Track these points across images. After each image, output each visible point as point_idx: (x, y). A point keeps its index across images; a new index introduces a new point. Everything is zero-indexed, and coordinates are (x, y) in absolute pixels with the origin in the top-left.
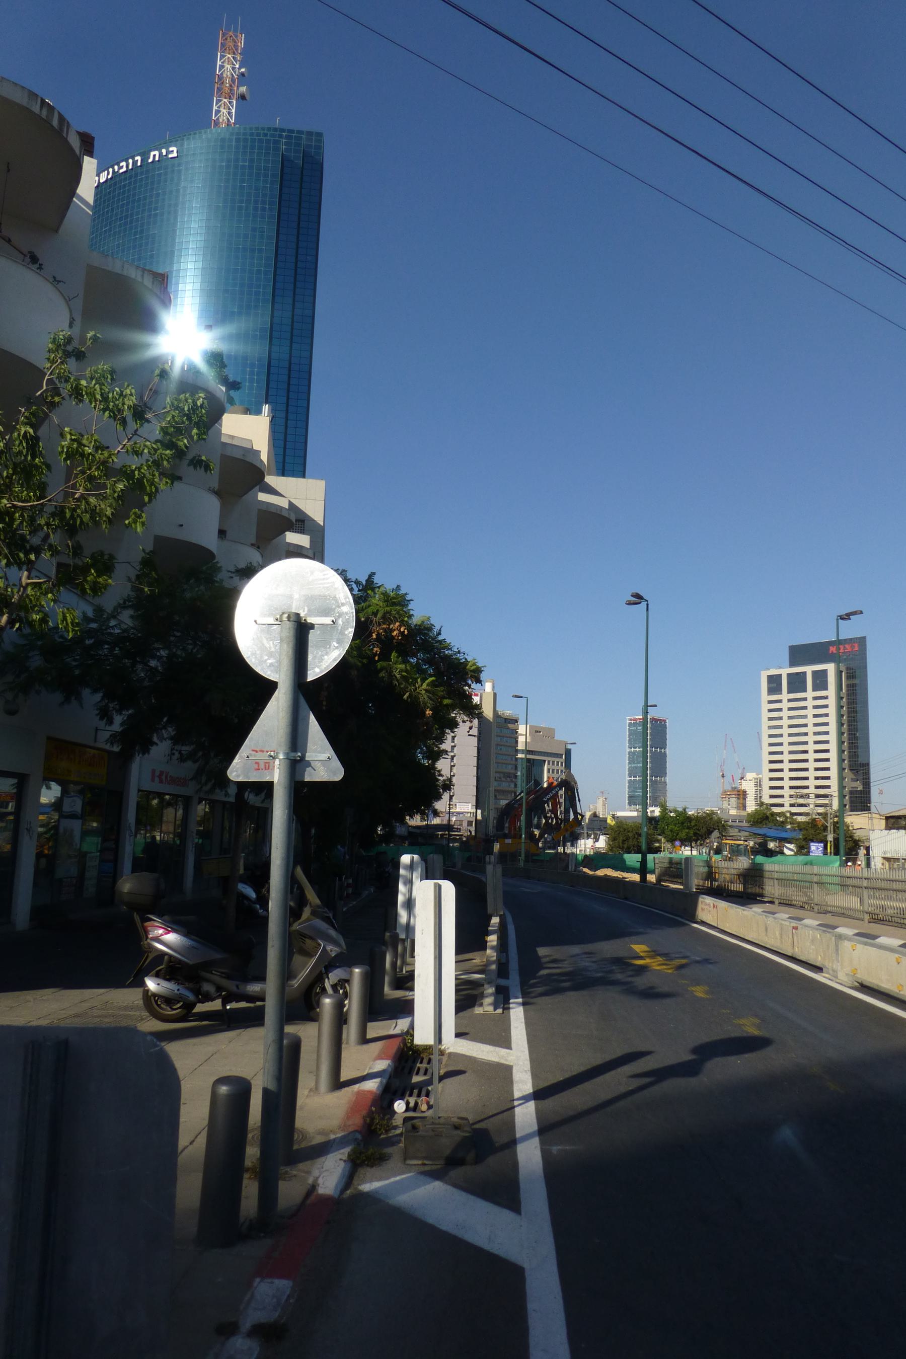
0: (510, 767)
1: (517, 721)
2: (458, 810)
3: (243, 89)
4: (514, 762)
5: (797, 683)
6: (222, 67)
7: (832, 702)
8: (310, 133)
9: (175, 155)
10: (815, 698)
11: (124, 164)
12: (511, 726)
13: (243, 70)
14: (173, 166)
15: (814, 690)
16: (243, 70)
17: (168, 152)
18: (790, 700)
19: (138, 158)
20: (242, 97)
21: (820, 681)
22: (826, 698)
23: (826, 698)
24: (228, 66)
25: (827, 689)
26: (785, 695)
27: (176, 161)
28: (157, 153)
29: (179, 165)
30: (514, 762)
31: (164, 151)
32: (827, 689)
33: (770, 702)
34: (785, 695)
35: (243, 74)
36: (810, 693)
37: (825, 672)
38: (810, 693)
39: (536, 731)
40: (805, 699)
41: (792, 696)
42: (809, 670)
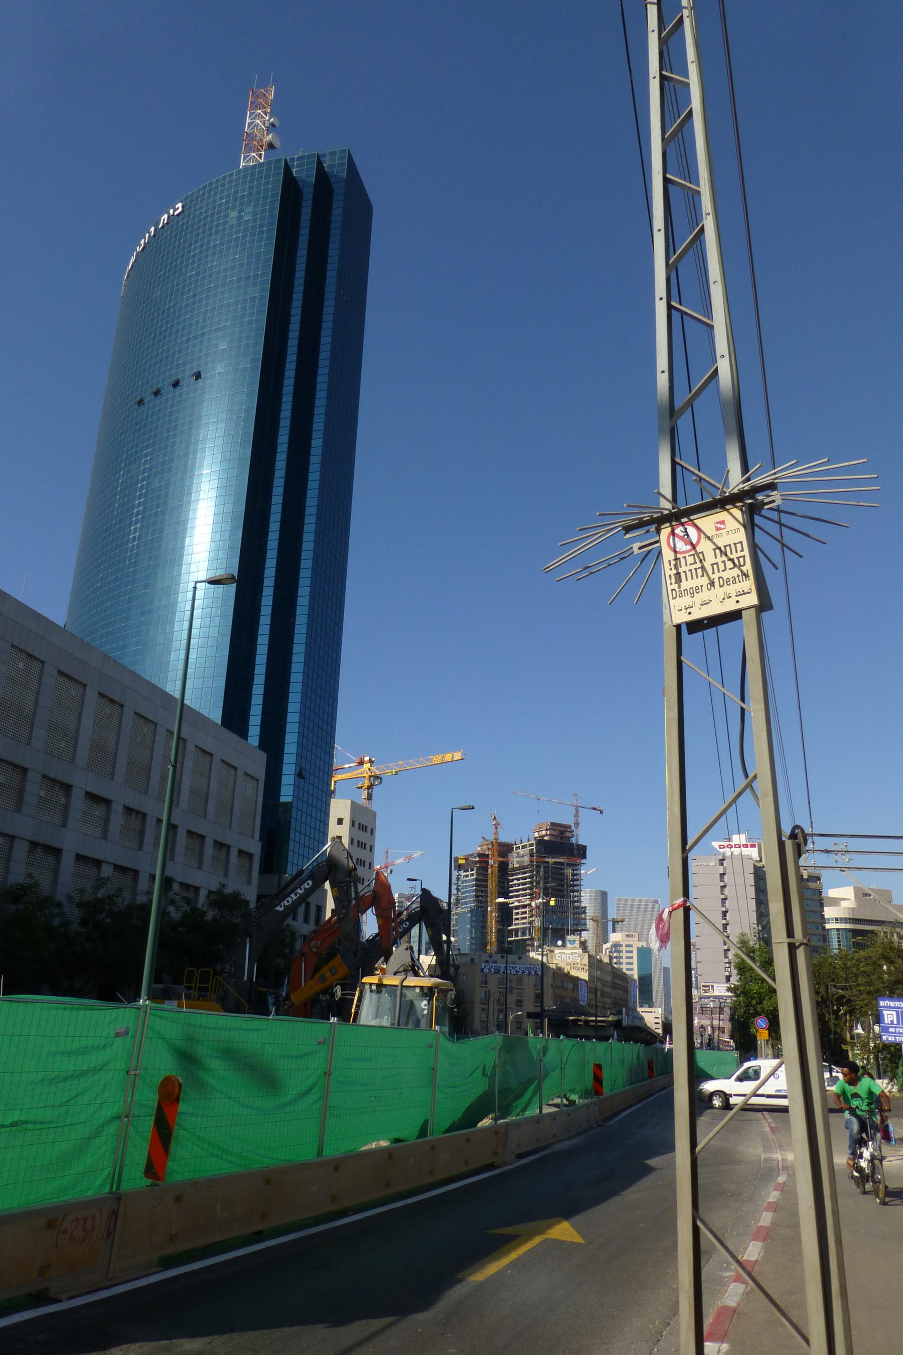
0: (816, 938)
1: (819, 878)
2: (716, 993)
3: (269, 138)
4: (820, 931)
6: (250, 124)
8: (333, 154)
9: (180, 210)
11: (143, 241)
12: (812, 885)
13: (272, 120)
14: (178, 222)
16: (272, 120)
17: (175, 210)
19: (152, 229)
20: (271, 146)
24: (257, 121)
27: (181, 217)
28: (166, 216)
29: (183, 219)
30: (820, 931)
31: (171, 211)
35: (273, 125)
39: (862, 895)
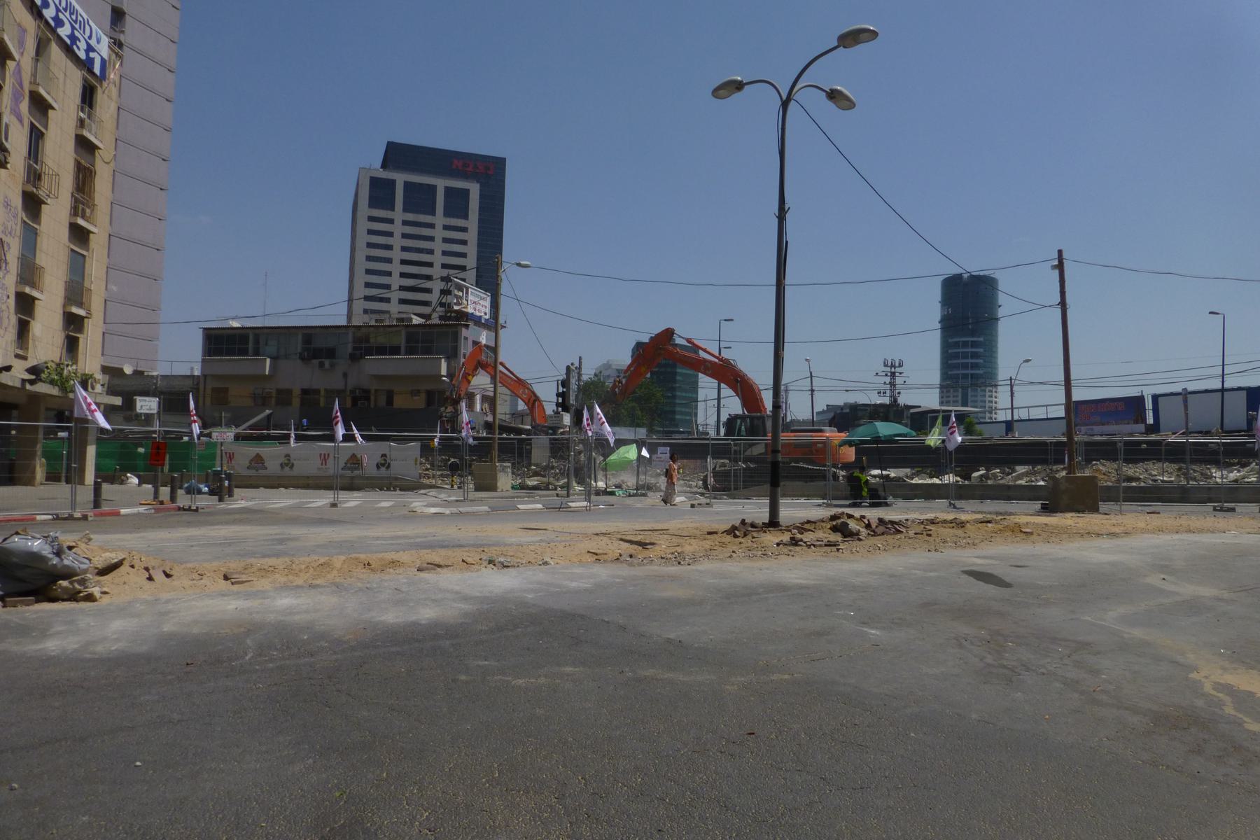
5: (420, 199)
7: (472, 236)
10: (446, 228)
15: (447, 213)
18: (405, 223)
21: (457, 204)
22: (464, 230)
23: (464, 230)
25: (466, 217)
26: (398, 214)
32: (466, 217)
33: (371, 219)
34: (398, 214)
36: (439, 219)
37: (465, 193)
38: (439, 219)
40: (432, 226)
41: (411, 217)
42: (441, 184)
